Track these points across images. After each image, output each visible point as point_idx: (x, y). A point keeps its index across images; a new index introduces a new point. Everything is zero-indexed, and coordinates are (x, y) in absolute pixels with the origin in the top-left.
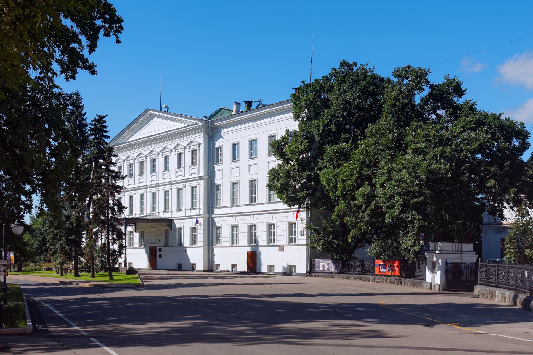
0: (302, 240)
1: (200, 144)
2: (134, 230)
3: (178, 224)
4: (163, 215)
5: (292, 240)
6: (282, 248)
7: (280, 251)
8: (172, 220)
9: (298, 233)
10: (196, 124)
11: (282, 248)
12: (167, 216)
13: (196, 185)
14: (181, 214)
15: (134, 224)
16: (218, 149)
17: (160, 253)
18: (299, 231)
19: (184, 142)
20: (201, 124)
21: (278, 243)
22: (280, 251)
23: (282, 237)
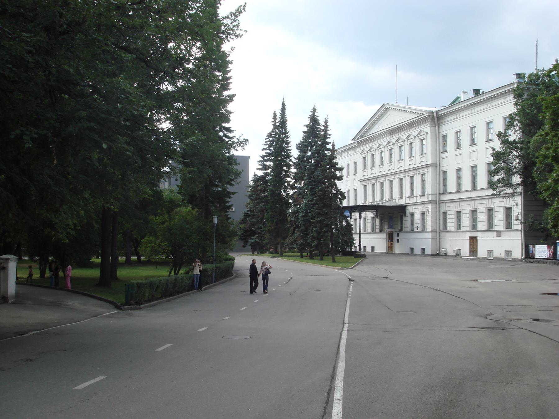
0: (517, 226)
1: (427, 133)
2: (376, 216)
3: (410, 210)
4: (399, 201)
5: (509, 226)
6: (499, 233)
7: (497, 236)
8: (406, 206)
9: (514, 218)
10: (423, 114)
11: (499, 233)
12: (402, 202)
13: (424, 173)
14: (413, 200)
15: (375, 211)
16: (443, 136)
17: (398, 238)
18: (515, 216)
19: (414, 132)
20: (427, 114)
21: (496, 228)
22: (497, 236)
23: (499, 223)
